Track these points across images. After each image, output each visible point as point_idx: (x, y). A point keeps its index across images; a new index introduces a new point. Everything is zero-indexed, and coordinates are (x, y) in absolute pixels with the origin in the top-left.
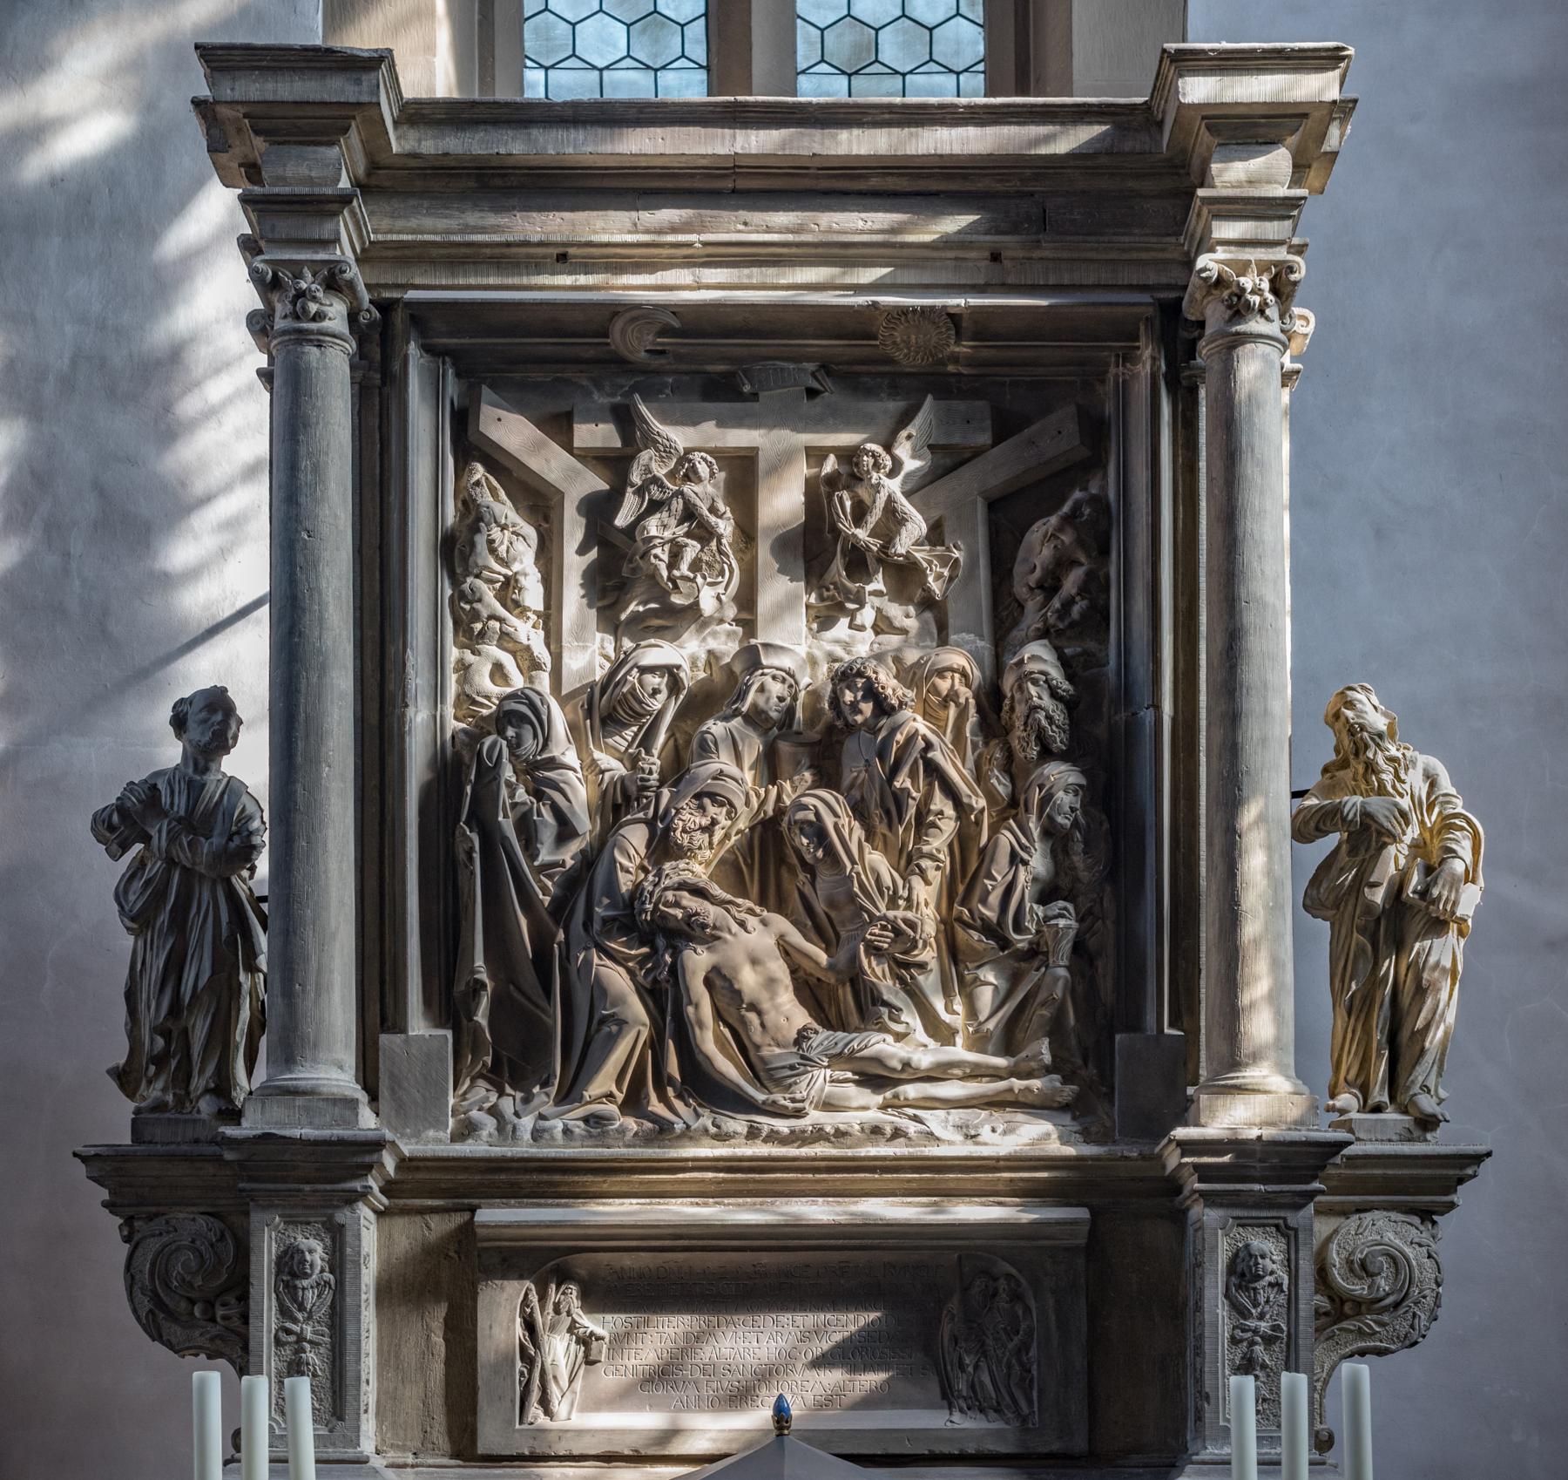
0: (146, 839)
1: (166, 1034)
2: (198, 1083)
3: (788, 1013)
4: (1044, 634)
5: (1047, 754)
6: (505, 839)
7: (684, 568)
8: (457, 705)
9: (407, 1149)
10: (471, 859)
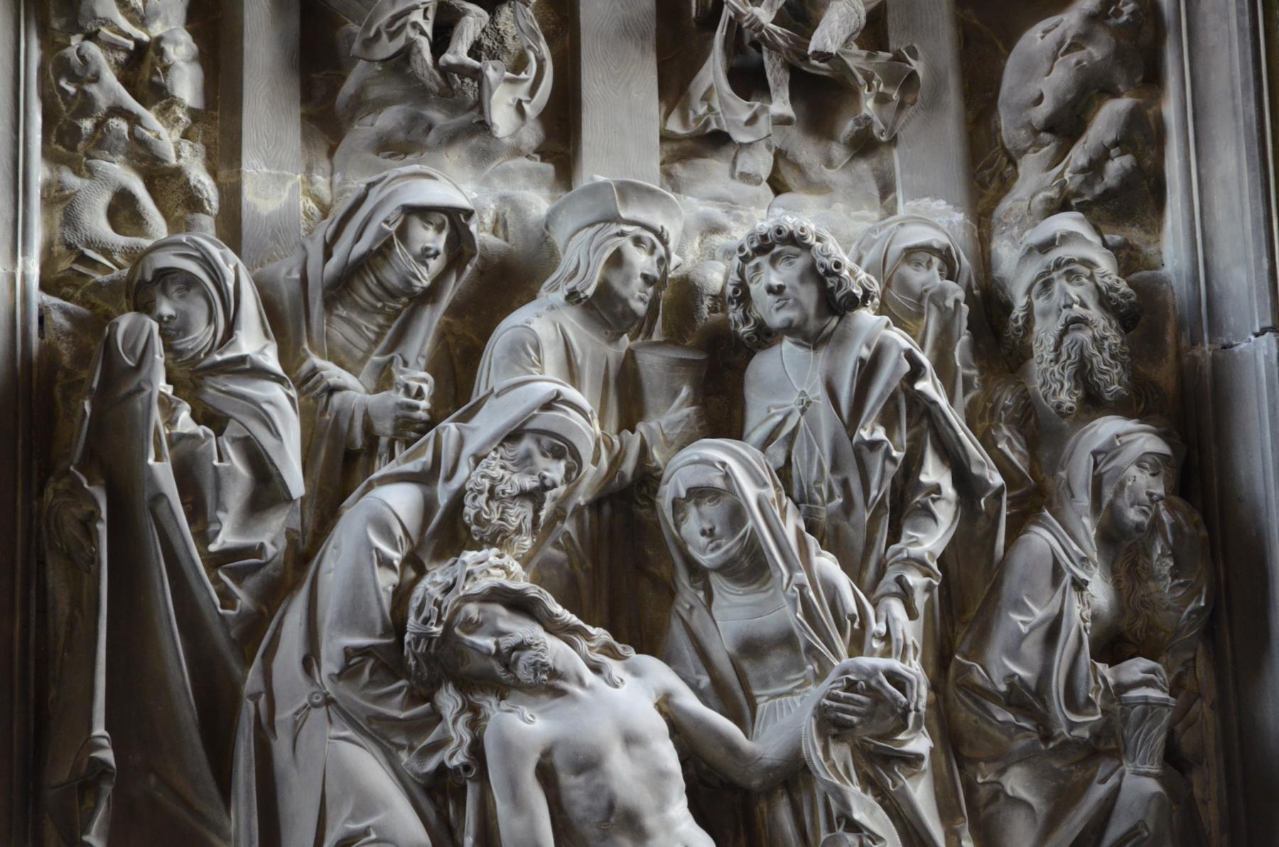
5: (1094, 402)
6: (160, 496)
7: (458, 53)
10: (91, 535)
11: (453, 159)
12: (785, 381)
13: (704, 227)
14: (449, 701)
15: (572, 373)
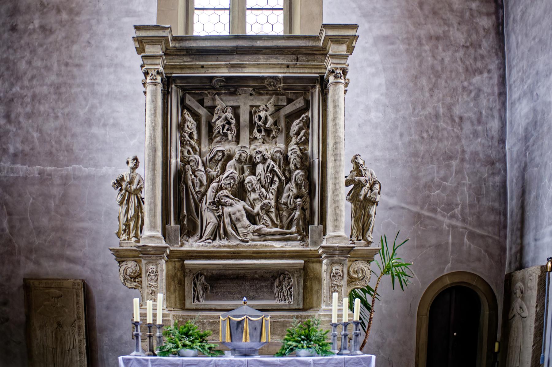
0: (121, 186)
1: (126, 225)
2: (132, 235)
4: (297, 144)
5: (297, 168)
7: (225, 131)
9: (171, 249)
11: (226, 143)
12: (260, 168)
13: (251, 149)
14: (220, 207)
15: (235, 169)
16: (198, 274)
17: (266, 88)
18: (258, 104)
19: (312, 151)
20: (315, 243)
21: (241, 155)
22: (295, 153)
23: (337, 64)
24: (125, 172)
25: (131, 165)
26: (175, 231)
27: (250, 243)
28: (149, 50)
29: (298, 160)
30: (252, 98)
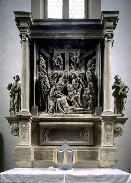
2: (16, 111)
3: (67, 104)
4: (90, 70)
5: (90, 81)
7: (58, 64)
8: (39, 77)
9: (33, 117)
12: (74, 81)
14: (56, 98)
15: (63, 81)
16: (46, 128)
17: (76, 45)
18: (73, 52)
19: (97, 74)
20: (98, 115)
21: (65, 75)
22: (89, 74)
23: (109, 31)
24: (13, 82)
25: (16, 79)
26: (36, 109)
27: (69, 114)
28: (22, 25)
29: (91, 77)
30: (70, 49)
